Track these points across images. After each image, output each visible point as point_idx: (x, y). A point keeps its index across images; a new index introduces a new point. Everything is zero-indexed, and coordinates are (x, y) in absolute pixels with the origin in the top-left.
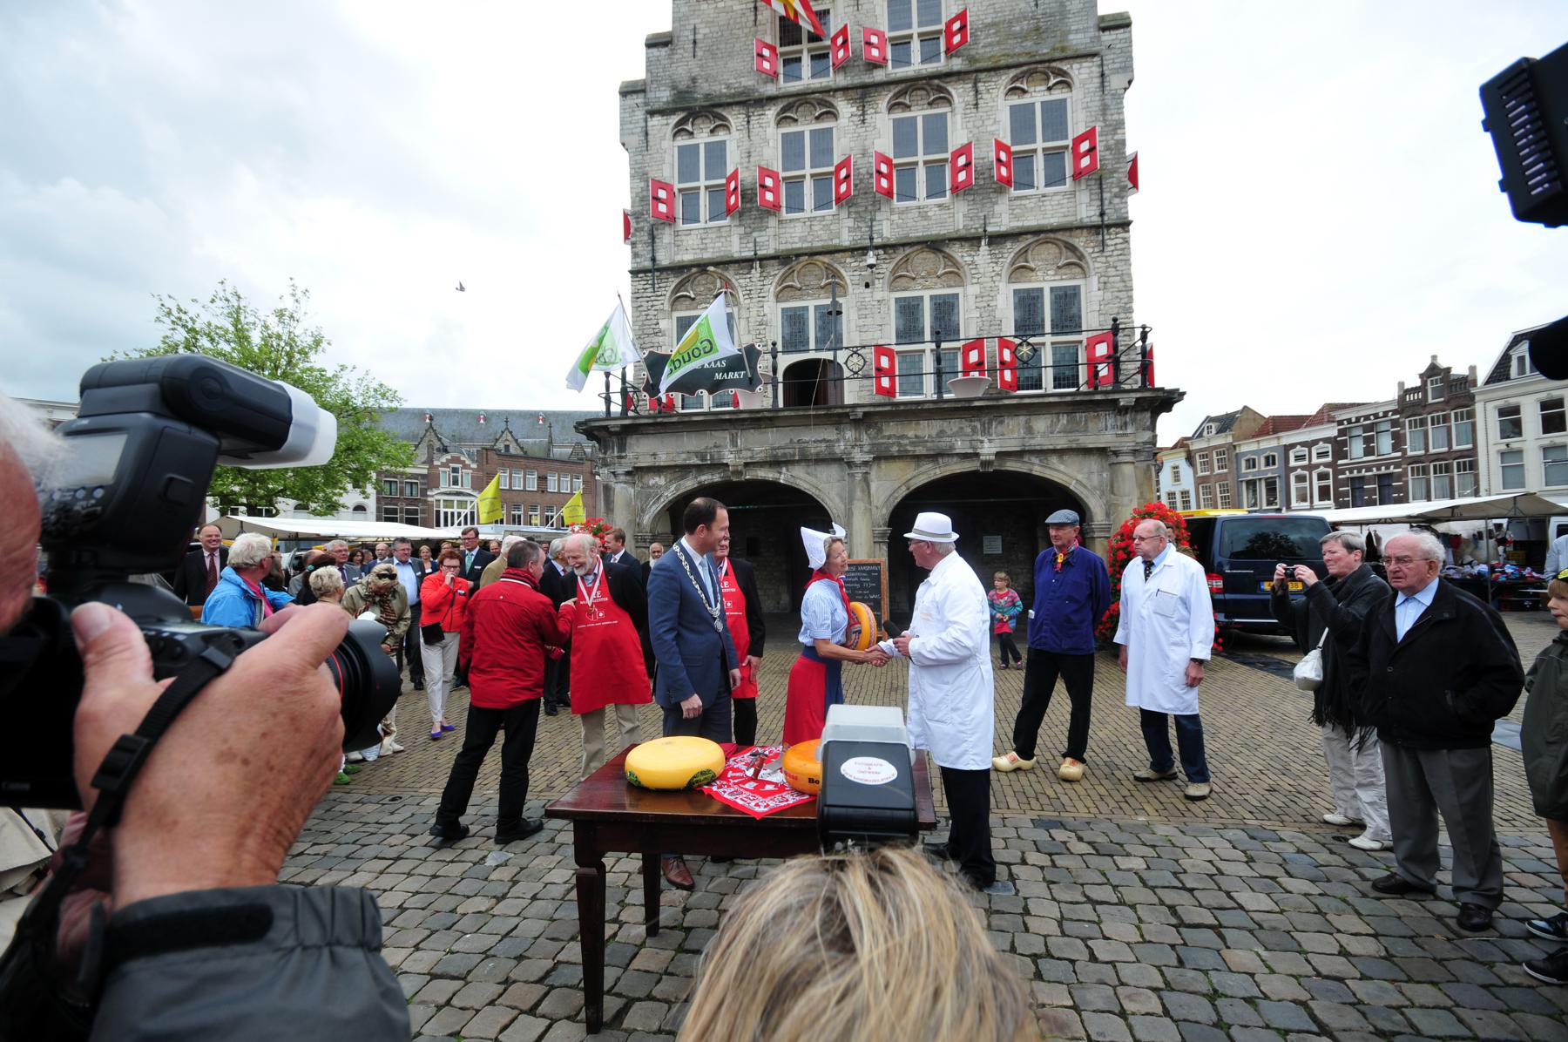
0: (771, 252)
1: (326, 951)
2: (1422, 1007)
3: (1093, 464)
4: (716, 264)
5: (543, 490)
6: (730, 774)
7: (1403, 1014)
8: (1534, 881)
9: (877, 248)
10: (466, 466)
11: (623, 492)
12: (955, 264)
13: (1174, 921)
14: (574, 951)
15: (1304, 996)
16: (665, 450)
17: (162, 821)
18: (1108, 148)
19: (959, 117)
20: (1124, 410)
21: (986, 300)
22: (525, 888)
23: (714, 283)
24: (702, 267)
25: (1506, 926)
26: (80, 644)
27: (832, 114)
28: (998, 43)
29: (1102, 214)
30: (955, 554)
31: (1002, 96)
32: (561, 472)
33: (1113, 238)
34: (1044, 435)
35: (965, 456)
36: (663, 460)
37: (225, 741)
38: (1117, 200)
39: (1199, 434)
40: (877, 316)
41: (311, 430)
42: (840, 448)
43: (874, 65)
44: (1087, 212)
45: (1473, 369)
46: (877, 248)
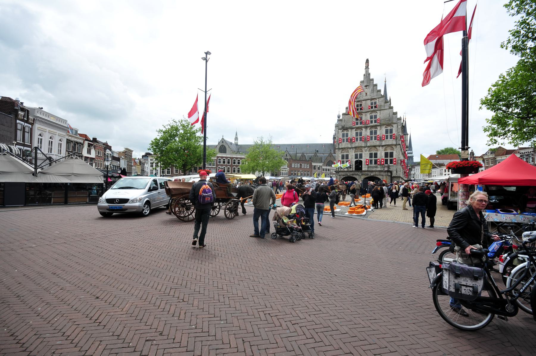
5: (301, 167)
11: (338, 177)
16: (343, 174)
39: (486, 154)
44: (394, 143)
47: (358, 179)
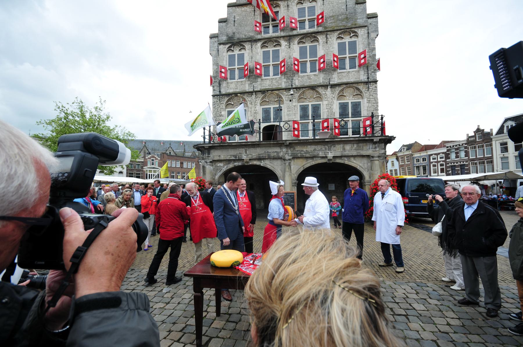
0: (259, 89)
1: (136, 311)
2: (474, 342)
3: (365, 160)
4: (241, 93)
6: (245, 262)
7: (468, 345)
8: (512, 301)
9: (294, 88)
10: (156, 159)
11: (209, 168)
12: (320, 94)
13: (392, 313)
14: (192, 321)
15: (435, 339)
16: (223, 154)
17: (90, 272)
18: (370, 57)
19: (321, 46)
20: (375, 143)
21: (330, 105)
22: (176, 300)
23: (240, 99)
24: (236, 94)
25: (502, 316)
26: (62, 220)
27: (279, 45)
28: (334, 22)
29: (368, 78)
30: (318, 190)
31: (335, 39)
32: (188, 161)
33: (372, 86)
34: (349, 151)
35: (323, 157)
36: (222, 158)
37: (107, 248)
38: (373, 74)
39: (400, 151)
40: (294, 111)
41: (124, 155)
42: (281, 154)
43: (293, 29)
44: (363, 77)
45: (491, 130)
46: (294, 88)
47: (278, 172)
